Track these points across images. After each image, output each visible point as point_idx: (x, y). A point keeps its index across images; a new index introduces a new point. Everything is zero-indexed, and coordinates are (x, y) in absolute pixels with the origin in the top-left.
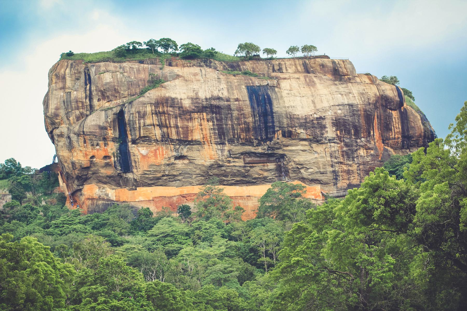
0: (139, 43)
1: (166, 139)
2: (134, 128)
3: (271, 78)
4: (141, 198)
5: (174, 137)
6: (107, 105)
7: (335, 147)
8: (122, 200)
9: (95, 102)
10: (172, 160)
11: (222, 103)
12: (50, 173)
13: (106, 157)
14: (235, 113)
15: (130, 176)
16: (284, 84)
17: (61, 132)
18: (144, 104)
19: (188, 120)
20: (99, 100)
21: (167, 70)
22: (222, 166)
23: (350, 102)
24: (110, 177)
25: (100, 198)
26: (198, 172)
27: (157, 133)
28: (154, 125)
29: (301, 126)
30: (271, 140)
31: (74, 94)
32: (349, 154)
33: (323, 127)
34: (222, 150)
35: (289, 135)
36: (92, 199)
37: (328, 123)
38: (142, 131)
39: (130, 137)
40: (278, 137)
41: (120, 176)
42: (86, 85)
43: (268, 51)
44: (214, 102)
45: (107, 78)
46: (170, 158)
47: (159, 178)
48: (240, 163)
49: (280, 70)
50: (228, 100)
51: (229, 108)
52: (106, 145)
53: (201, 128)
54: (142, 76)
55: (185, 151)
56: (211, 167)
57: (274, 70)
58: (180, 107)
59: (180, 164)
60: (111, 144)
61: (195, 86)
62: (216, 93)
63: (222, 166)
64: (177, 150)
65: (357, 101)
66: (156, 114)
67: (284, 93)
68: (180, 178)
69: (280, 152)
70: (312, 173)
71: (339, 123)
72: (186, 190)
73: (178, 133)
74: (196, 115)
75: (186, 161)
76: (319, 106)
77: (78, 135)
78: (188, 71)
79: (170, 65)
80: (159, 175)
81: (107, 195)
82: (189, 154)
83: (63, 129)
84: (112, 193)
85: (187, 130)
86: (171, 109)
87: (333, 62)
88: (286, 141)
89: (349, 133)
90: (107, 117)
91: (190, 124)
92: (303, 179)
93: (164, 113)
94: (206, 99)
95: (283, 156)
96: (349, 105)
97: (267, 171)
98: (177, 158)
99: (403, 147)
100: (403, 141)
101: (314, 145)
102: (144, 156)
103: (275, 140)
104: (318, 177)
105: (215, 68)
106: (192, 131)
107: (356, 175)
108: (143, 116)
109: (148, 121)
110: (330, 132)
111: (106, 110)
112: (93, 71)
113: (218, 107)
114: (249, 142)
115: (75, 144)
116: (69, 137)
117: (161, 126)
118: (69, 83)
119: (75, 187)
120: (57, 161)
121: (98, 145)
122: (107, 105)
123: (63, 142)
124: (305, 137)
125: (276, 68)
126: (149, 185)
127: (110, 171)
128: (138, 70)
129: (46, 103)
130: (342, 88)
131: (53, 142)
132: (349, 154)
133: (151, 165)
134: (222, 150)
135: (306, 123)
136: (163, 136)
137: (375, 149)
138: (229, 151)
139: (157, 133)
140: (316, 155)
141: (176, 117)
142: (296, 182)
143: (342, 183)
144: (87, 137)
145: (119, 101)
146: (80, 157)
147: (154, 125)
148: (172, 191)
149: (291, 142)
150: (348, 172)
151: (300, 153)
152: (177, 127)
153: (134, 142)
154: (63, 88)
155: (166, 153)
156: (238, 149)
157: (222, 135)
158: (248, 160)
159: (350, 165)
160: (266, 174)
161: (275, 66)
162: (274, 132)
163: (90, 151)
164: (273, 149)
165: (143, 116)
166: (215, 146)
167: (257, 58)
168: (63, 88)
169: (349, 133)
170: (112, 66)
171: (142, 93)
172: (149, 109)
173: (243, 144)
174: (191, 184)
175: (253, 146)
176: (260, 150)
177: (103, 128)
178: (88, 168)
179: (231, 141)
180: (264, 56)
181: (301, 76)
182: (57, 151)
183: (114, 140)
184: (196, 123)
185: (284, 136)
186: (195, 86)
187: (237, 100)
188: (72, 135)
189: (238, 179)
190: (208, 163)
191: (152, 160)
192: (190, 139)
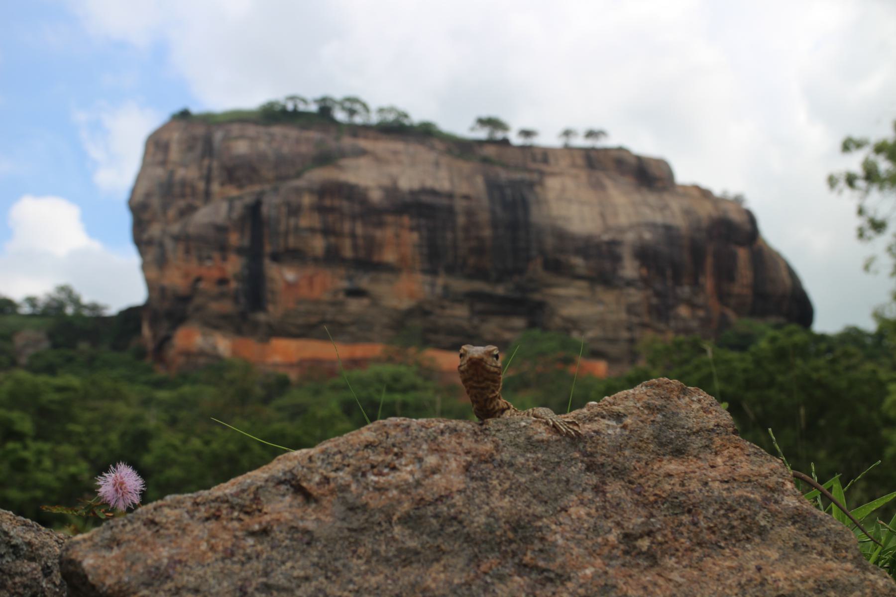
0: (304, 101)
1: (332, 257)
3: (531, 171)
4: (277, 359)
5: (348, 253)
7: (635, 296)
9: (215, 187)
10: (341, 296)
12: (131, 315)
13: (223, 281)
14: (461, 220)
15: (261, 317)
16: (553, 184)
18: (299, 191)
21: (347, 142)
24: (225, 317)
25: (202, 353)
31: (181, 173)
32: (662, 311)
33: (617, 259)
35: (557, 267)
36: (187, 354)
37: (626, 254)
40: (536, 268)
41: (243, 316)
43: (527, 133)
44: (425, 199)
45: (241, 148)
46: (336, 292)
50: (450, 196)
52: (224, 259)
53: (399, 241)
54: (304, 149)
55: (364, 282)
56: (409, 313)
57: (534, 160)
59: (355, 305)
61: (394, 170)
62: (430, 183)
64: (350, 278)
65: (679, 222)
67: (551, 195)
68: (353, 329)
69: (537, 297)
70: (592, 340)
71: (644, 254)
72: (360, 351)
73: (355, 247)
74: (390, 219)
75: (365, 301)
76: (611, 222)
78: (383, 146)
80: (313, 320)
81: (215, 348)
83: (155, 230)
84: (223, 345)
85: (372, 245)
90: (231, 208)
91: (378, 234)
94: (412, 193)
101: (599, 289)
102: (290, 285)
105: (432, 148)
108: (294, 211)
109: (304, 222)
110: (630, 269)
111: (231, 200)
112: (218, 136)
114: (480, 274)
116: (161, 245)
117: (327, 232)
119: (162, 333)
121: (209, 258)
123: (153, 252)
125: (539, 157)
127: (227, 306)
128: (298, 141)
130: (652, 198)
132: (662, 311)
134: (433, 285)
135: (589, 247)
138: (446, 288)
139: (318, 244)
140: (600, 308)
145: (257, 188)
146: (175, 279)
147: (312, 230)
151: (574, 302)
152: (353, 236)
153: (276, 258)
155: (329, 283)
156: (460, 285)
157: (434, 258)
158: (479, 306)
161: (536, 159)
163: (194, 267)
165: (294, 211)
166: (420, 277)
167: (505, 142)
168: (164, 163)
170: (252, 130)
171: (298, 175)
172: (307, 200)
173: (471, 277)
174: (369, 340)
177: (221, 229)
179: (451, 270)
180: (516, 139)
181: (583, 175)
183: (240, 251)
186: (394, 170)
187: (466, 197)
190: (405, 304)
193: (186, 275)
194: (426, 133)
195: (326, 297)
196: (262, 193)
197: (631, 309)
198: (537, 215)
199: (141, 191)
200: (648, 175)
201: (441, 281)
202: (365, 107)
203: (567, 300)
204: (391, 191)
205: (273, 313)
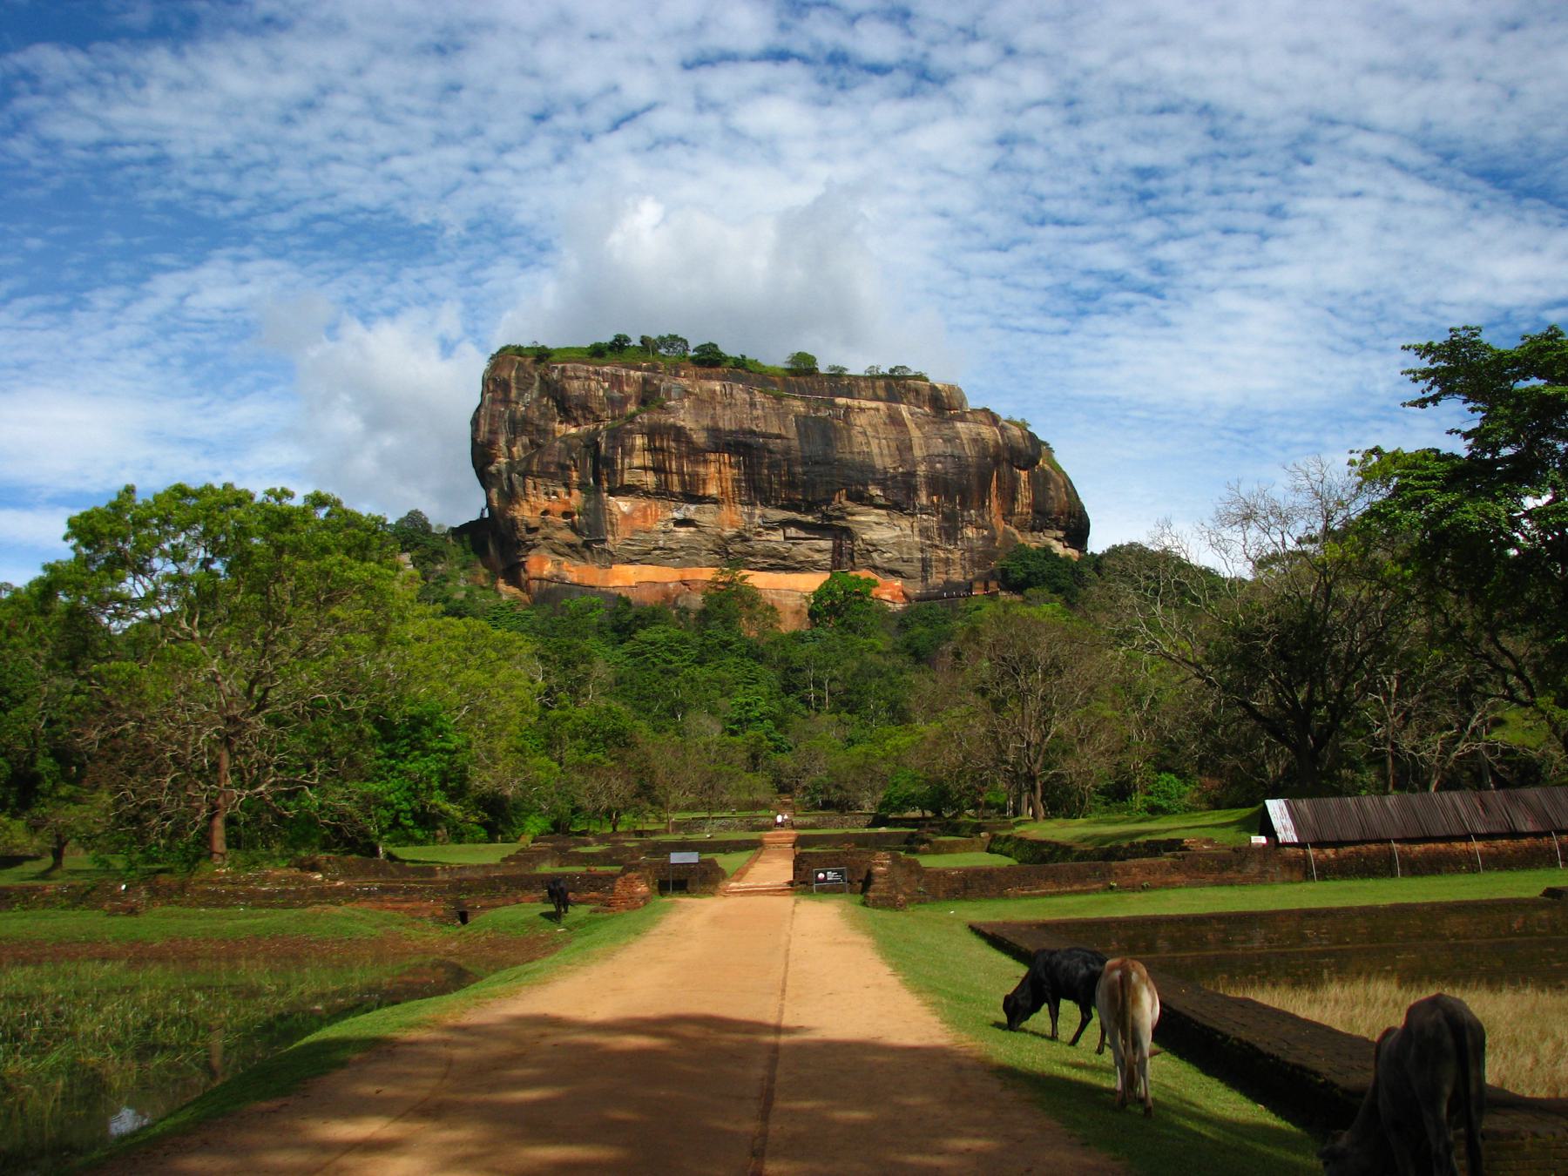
1: (662, 493)
2: (614, 472)
4: (618, 583)
5: (677, 489)
6: (573, 430)
8: (586, 582)
10: (671, 525)
11: (751, 440)
13: (566, 515)
17: (499, 471)
19: (697, 462)
20: (561, 422)
22: (748, 540)
23: (956, 452)
26: (710, 546)
27: (650, 479)
28: (645, 468)
29: (878, 483)
30: (828, 502)
33: (912, 490)
34: (751, 515)
36: (540, 579)
38: (626, 476)
39: (606, 485)
40: (841, 500)
42: (541, 396)
44: (741, 438)
45: (575, 387)
47: (648, 553)
48: (777, 536)
49: (850, 395)
50: (764, 435)
51: (765, 448)
55: (690, 511)
56: (732, 539)
58: (689, 441)
59: (682, 532)
60: (576, 492)
63: (748, 540)
65: (970, 451)
66: (649, 450)
69: (843, 524)
70: (890, 560)
71: (937, 484)
72: (691, 573)
73: (683, 483)
74: (712, 457)
77: (524, 475)
79: (677, 375)
82: (697, 517)
86: (672, 444)
87: (933, 388)
88: (851, 506)
89: (952, 500)
91: (701, 470)
92: (875, 568)
93: (662, 449)
94: (731, 432)
95: (847, 532)
96: (952, 456)
97: (819, 551)
98: (680, 523)
99: (1033, 529)
100: (1034, 519)
102: (626, 516)
103: (835, 504)
104: (897, 566)
106: (704, 482)
107: (958, 567)
109: (637, 462)
113: (748, 446)
115: (519, 490)
116: (509, 479)
117: (658, 469)
118: (514, 393)
120: (486, 515)
121: (555, 493)
122: (573, 430)
124: (883, 501)
126: (631, 562)
129: (475, 422)
131: (483, 485)
132: (950, 530)
133: (634, 532)
136: (658, 486)
137: (990, 528)
138: (763, 516)
140: (898, 532)
141: (680, 457)
142: (864, 574)
143: (936, 579)
144: (539, 480)
147: (645, 468)
148: (668, 575)
149: (859, 509)
150: (947, 562)
152: (680, 473)
153: (612, 493)
154: (506, 401)
158: (792, 532)
159: (950, 551)
160: (817, 556)
162: (834, 492)
163: (543, 503)
164: (830, 518)
165: (629, 452)
169: (951, 500)
173: (783, 508)
174: (698, 565)
175: (800, 512)
176: (810, 519)
178: (536, 530)
179: (766, 503)
182: (489, 500)
183: (582, 486)
184: (712, 469)
185: (848, 498)
187: (779, 436)
188: (515, 476)
189: (773, 561)
190: (729, 532)
191: (639, 524)
192: (701, 493)
193: (533, 509)
194: (740, 363)
195: (659, 526)
196: (597, 432)
197: (924, 532)
198: (842, 452)
199: (484, 429)
200: (942, 405)
201: (757, 512)
202: (686, 342)
203: (869, 526)
204: (714, 431)
205: (613, 542)
